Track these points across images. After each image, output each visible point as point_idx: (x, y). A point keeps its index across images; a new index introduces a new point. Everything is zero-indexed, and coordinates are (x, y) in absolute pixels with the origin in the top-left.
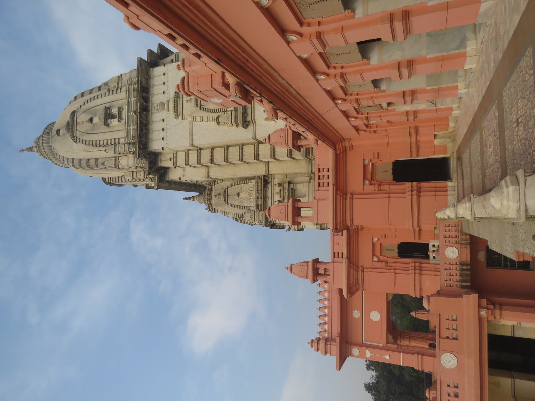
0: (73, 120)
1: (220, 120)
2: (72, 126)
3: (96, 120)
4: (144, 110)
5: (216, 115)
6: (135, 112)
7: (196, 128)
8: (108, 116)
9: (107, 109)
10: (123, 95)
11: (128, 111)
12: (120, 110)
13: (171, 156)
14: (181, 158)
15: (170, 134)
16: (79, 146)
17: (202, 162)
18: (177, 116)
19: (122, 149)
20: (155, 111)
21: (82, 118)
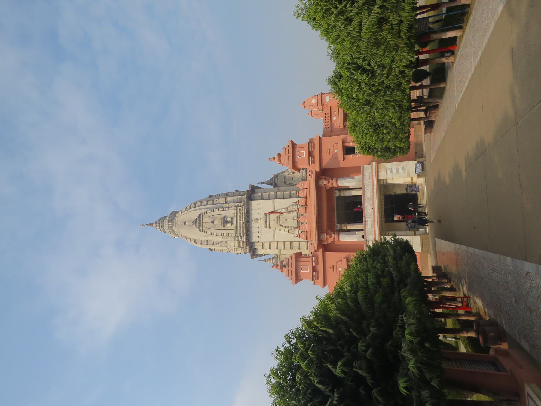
0: (200, 220)
1: (290, 231)
2: (199, 224)
3: (216, 222)
4: (248, 222)
5: (288, 229)
6: (243, 223)
7: (277, 234)
8: (225, 222)
9: (224, 217)
10: (233, 212)
11: (237, 220)
12: (232, 218)
13: (261, 244)
14: (267, 245)
15: (262, 234)
16: (203, 234)
17: (279, 248)
18: (266, 227)
19: (233, 239)
20: (253, 222)
21: (205, 219)
